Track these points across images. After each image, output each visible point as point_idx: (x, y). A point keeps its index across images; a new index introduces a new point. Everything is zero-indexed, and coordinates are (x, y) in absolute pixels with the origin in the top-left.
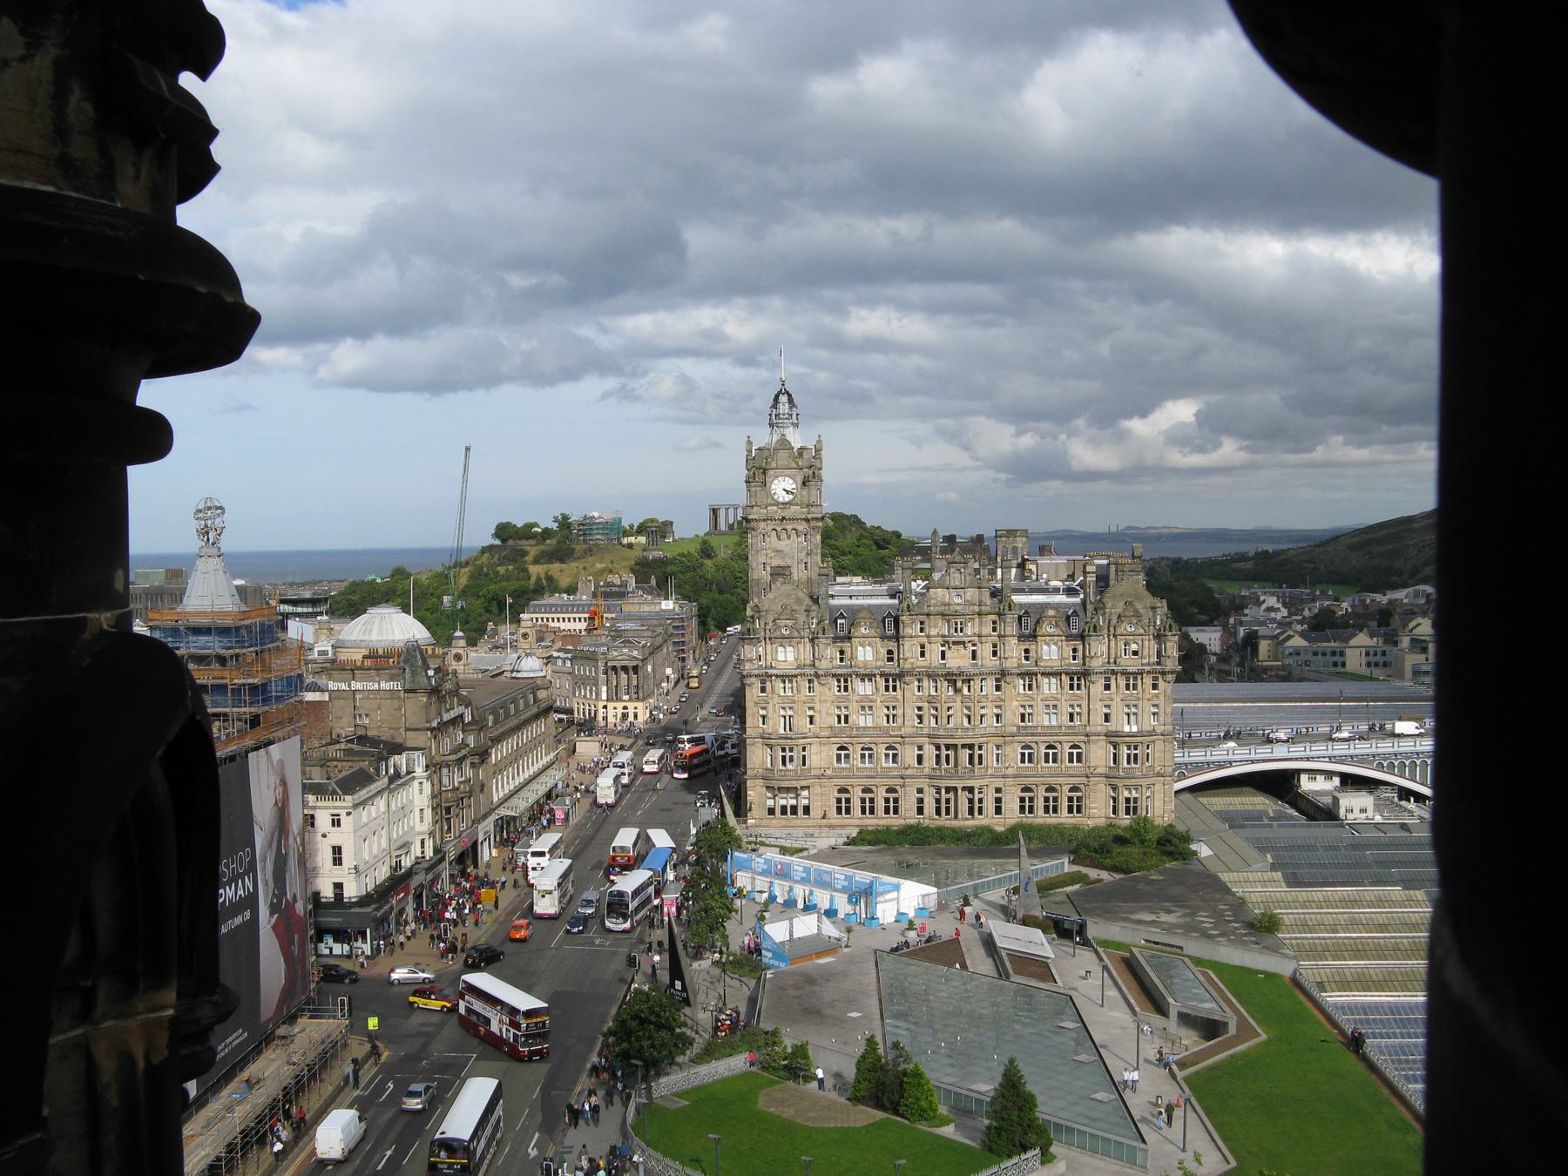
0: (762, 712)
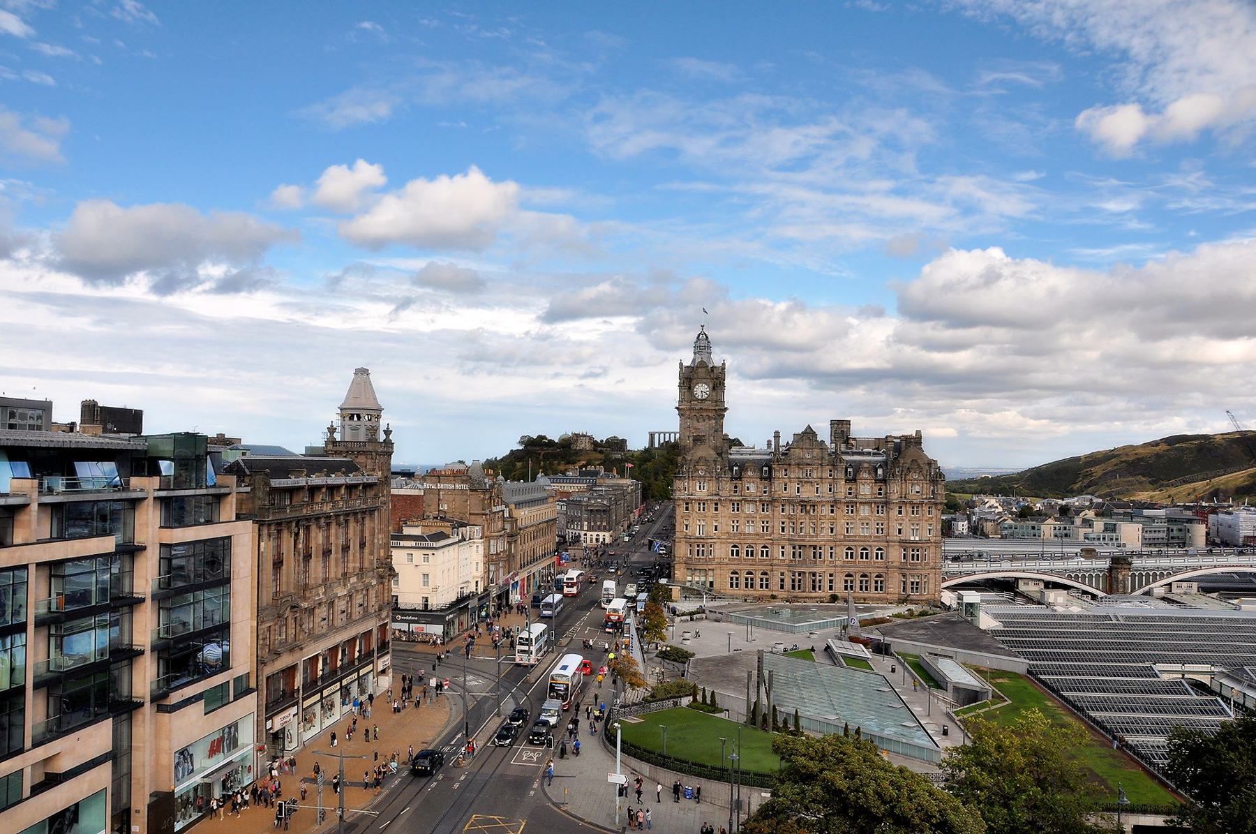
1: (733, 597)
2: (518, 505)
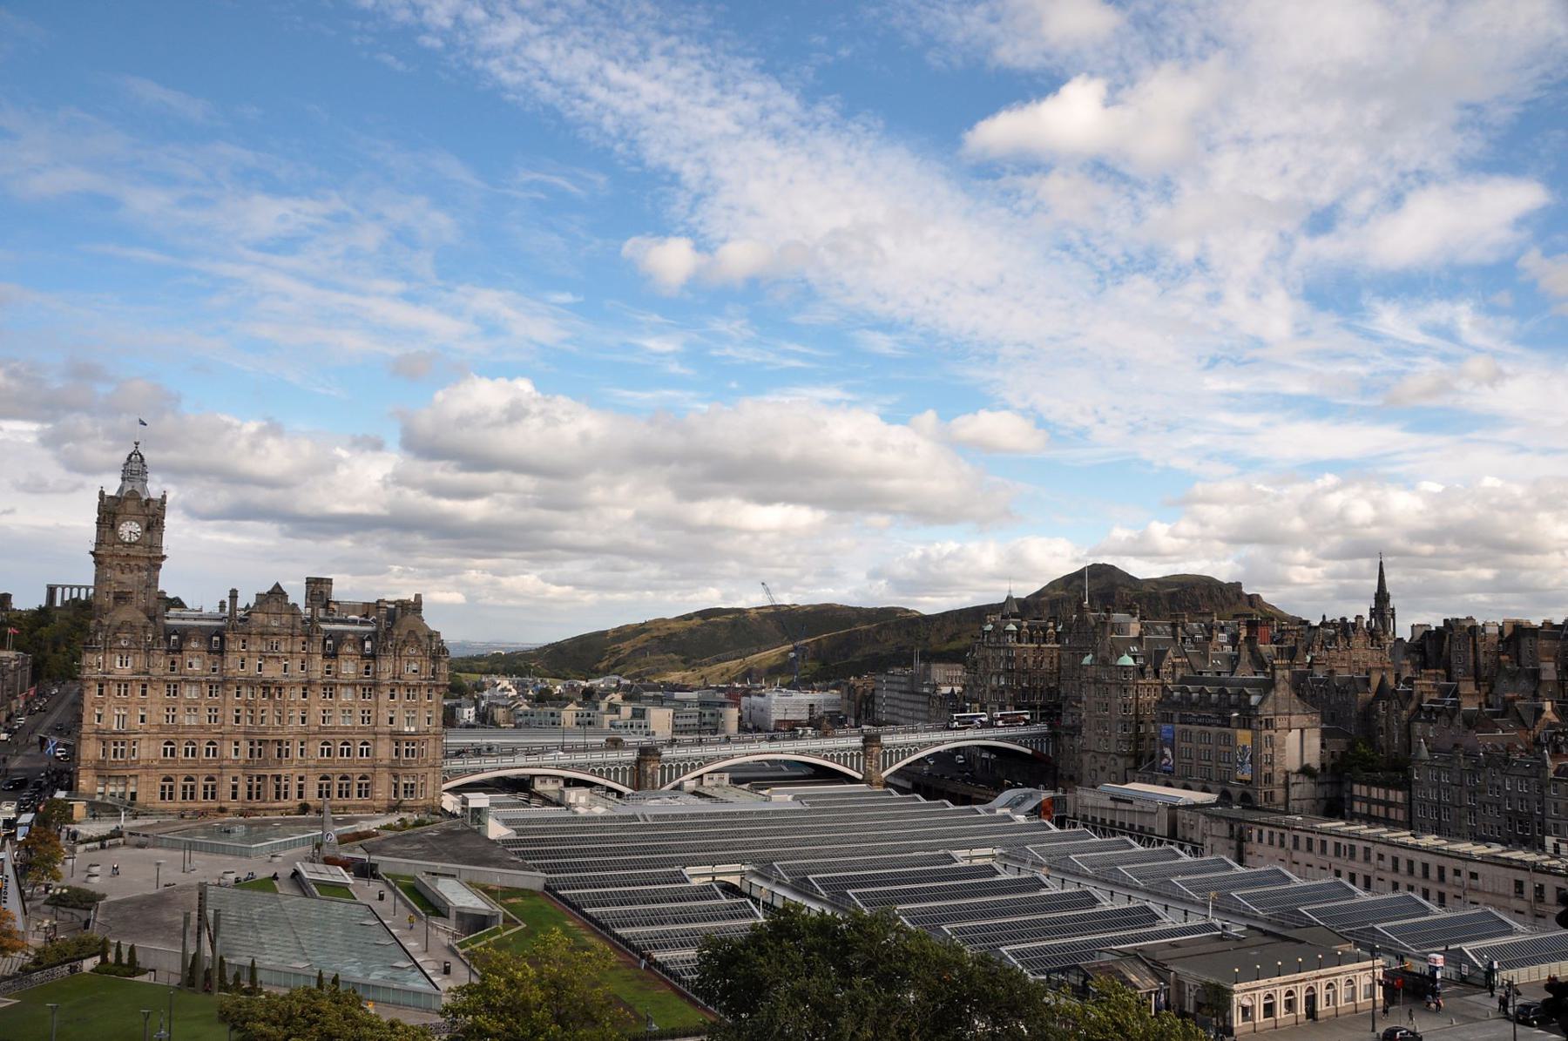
1: (164, 813)
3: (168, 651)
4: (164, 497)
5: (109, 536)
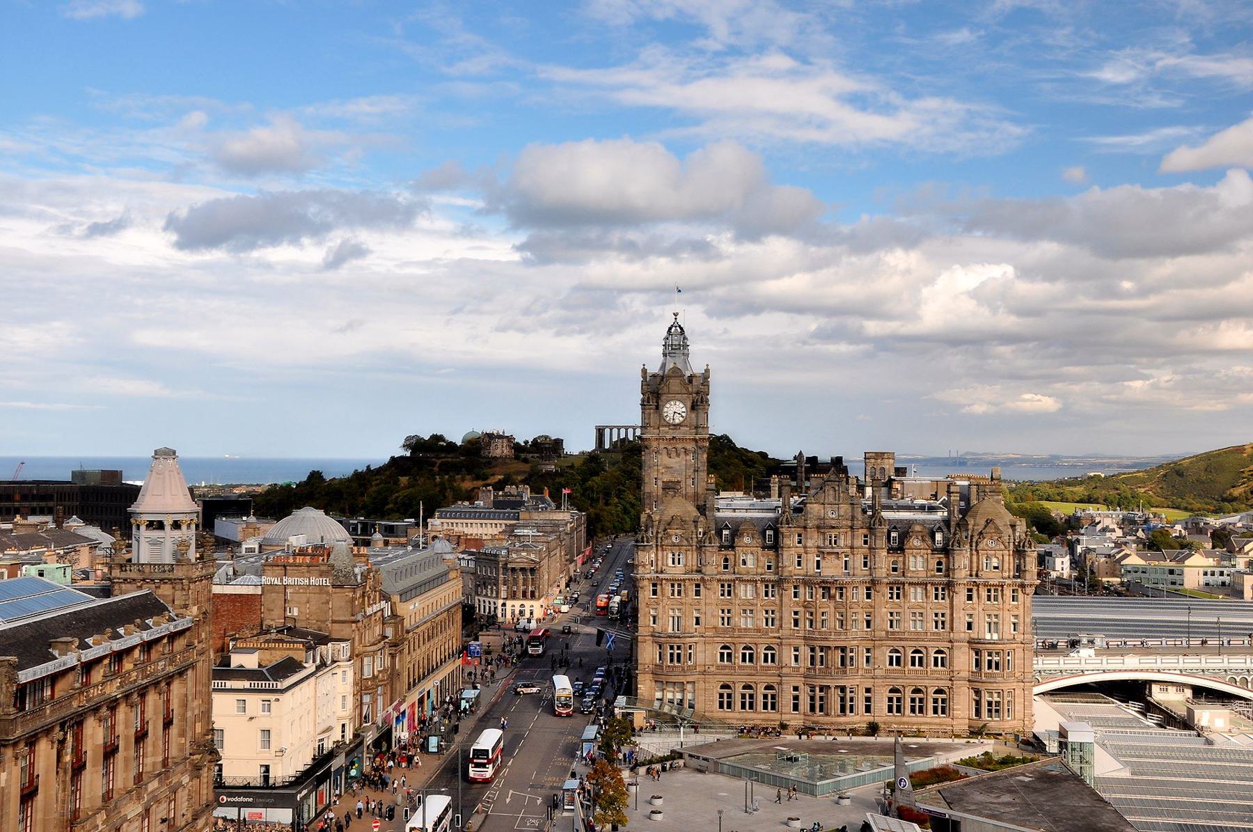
0: (652, 612)
1: (725, 725)
2: (406, 595)
3: (721, 547)
4: (707, 371)
5: (654, 419)
